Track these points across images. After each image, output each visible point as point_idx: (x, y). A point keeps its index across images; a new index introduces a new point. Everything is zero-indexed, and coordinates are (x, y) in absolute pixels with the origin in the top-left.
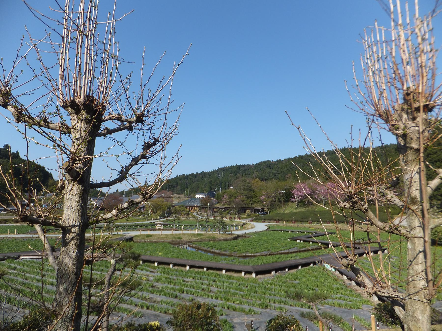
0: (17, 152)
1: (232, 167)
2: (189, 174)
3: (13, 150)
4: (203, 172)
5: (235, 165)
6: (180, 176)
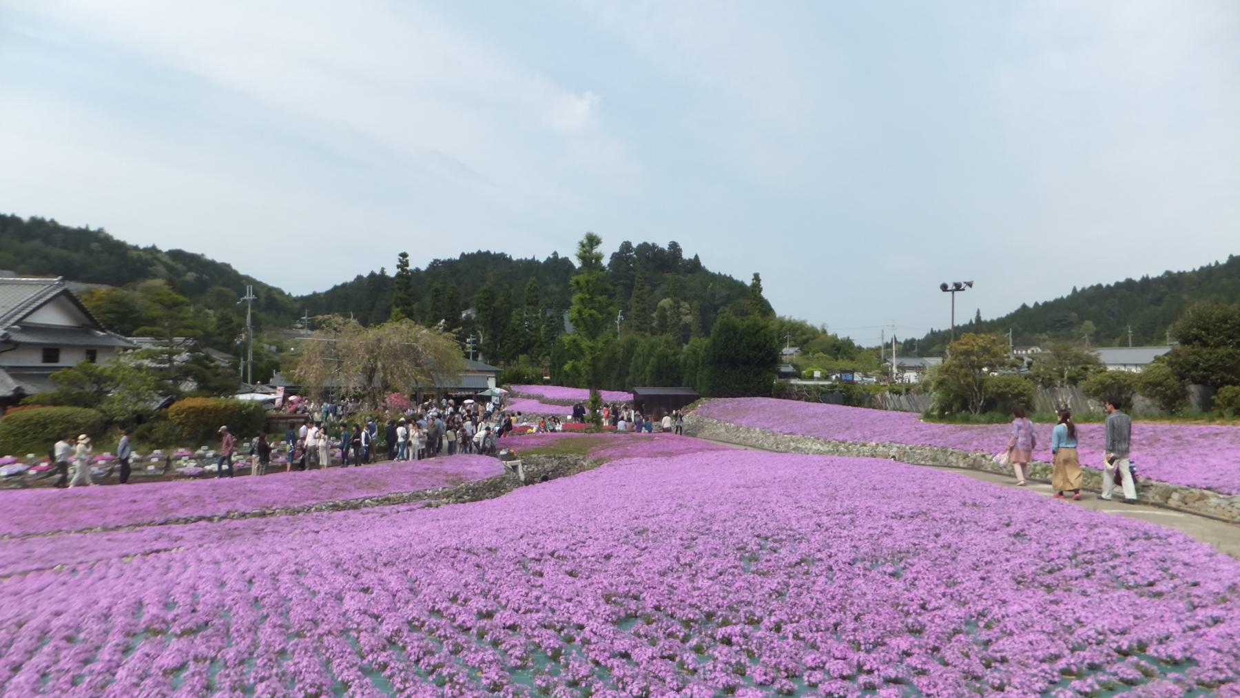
0: (696, 257)
3: (687, 255)
4: (1168, 273)
6: (1083, 290)
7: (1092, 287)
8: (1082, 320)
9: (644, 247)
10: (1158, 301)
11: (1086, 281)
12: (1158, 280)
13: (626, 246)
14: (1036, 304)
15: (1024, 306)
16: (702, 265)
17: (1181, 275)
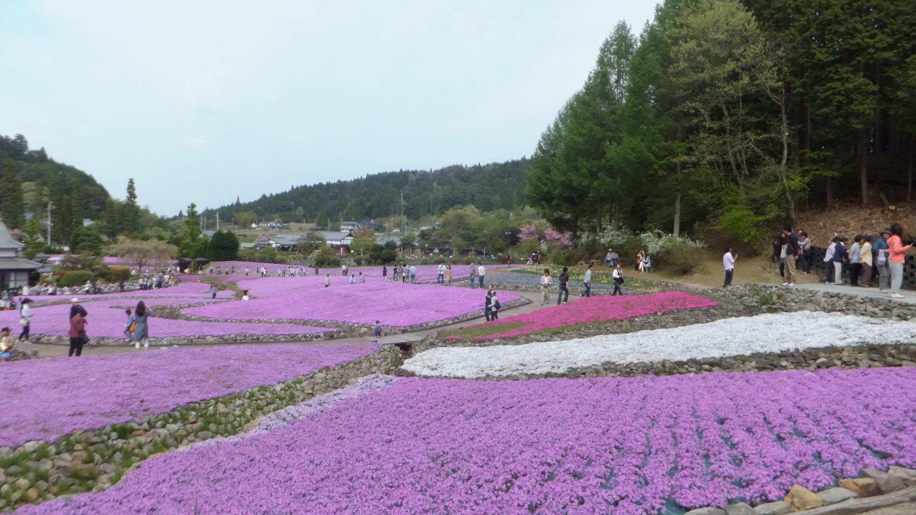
1: (393, 175)
2: (315, 185)
4: (339, 181)
5: (398, 171)
6: (297, 188)
7: (302, 186)
8: (297, 207)
10: (335, 198)
11: (299, 183)
12: (335, 185)
14: (271, 194)
15: (264, 196)
17: (345, 182)
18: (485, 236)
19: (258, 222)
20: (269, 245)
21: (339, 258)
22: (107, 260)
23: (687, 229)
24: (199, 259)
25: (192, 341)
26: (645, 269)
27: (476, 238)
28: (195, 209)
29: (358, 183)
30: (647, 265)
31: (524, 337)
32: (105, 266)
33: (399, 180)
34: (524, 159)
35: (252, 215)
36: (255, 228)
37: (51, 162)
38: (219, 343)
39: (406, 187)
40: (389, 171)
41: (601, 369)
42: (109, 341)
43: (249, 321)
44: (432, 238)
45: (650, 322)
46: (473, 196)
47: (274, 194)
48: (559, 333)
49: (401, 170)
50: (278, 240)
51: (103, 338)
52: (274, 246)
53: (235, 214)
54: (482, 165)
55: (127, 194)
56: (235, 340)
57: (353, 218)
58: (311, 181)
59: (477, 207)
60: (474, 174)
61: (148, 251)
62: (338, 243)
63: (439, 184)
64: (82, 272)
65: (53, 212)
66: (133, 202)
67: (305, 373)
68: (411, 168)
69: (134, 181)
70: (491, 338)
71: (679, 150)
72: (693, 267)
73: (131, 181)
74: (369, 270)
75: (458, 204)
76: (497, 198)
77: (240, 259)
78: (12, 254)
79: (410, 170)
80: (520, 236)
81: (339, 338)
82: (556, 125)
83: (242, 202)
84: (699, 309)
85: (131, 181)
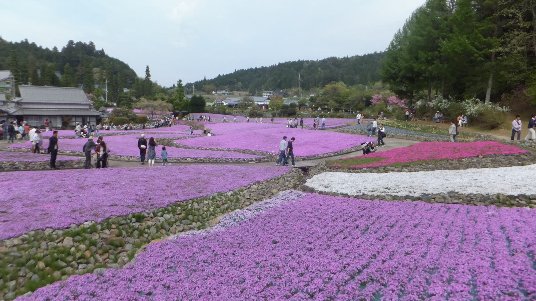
1: (294, 63)
2: (248, 69)
4: (262, 67)
5: (297, 60)
6: (238, 71)
7: (241, 70)
8: (238, 82)
9: (80, 44)
11: (238, 68)
12: (260, 69)
13: (71, 42)
14: (223, 75)
15: (219, 75)
16: (106, 54)
17: (266, 67)
18: (350, 101)
19: (215, 91)
20: (222, 104)
21: (262, 112)
22: (135, 111)
23: (495, 99)
24: (184, 111)
25: (179, 160)
26: (462, 125)
27: (344, 101)
28: (181, 83)
29: (273, 68)
30: (464, 122)
31: (383, 167)
32: (134, 115)
33: (298, 66)
34: (375, 53)
35: (213, 87)
36: (214, 94)
37: (107, 57)
38: (195, 162)
39: (302, 70)
40: (292, 61)
41: (447, 196)
42: (134, 158)
43: (211, 149)
44: (317, 101)
45: (474, 162)
46: (342, 76)
47: (225, 75)
48: (407, 166)
49: (299, 60)
50: (227, 101)
51: (131, 157)
52: (225, 104)
53: (203, 86)
54: (349, 57)
55: (146, 75)
56: (204, 161)
57: (270, 89)
58: (246, 67)
59: (345, 83)
60: (344, 62)
61: (156, 106)
62: (262, 103)
63: (322, 69)
64: (122, 118)
65: (108, 84)
66: (149, 79)
67: (245, 185)
68: (305, 59)
69: (149, 67)
70: (361, 167)
71: (495, 44)
72: (500, 124)
73: (148, 67)
74: (280, 120)
75: (334, 80)
76: (357, 77)
77: (206, 112)
78: (88, 107)
79: (305, 60)
80: (372, 101)
81: (264, 162)
82: (404, 29)
83: (207, 79)
84: (512, 155)
85: (148, 67)
